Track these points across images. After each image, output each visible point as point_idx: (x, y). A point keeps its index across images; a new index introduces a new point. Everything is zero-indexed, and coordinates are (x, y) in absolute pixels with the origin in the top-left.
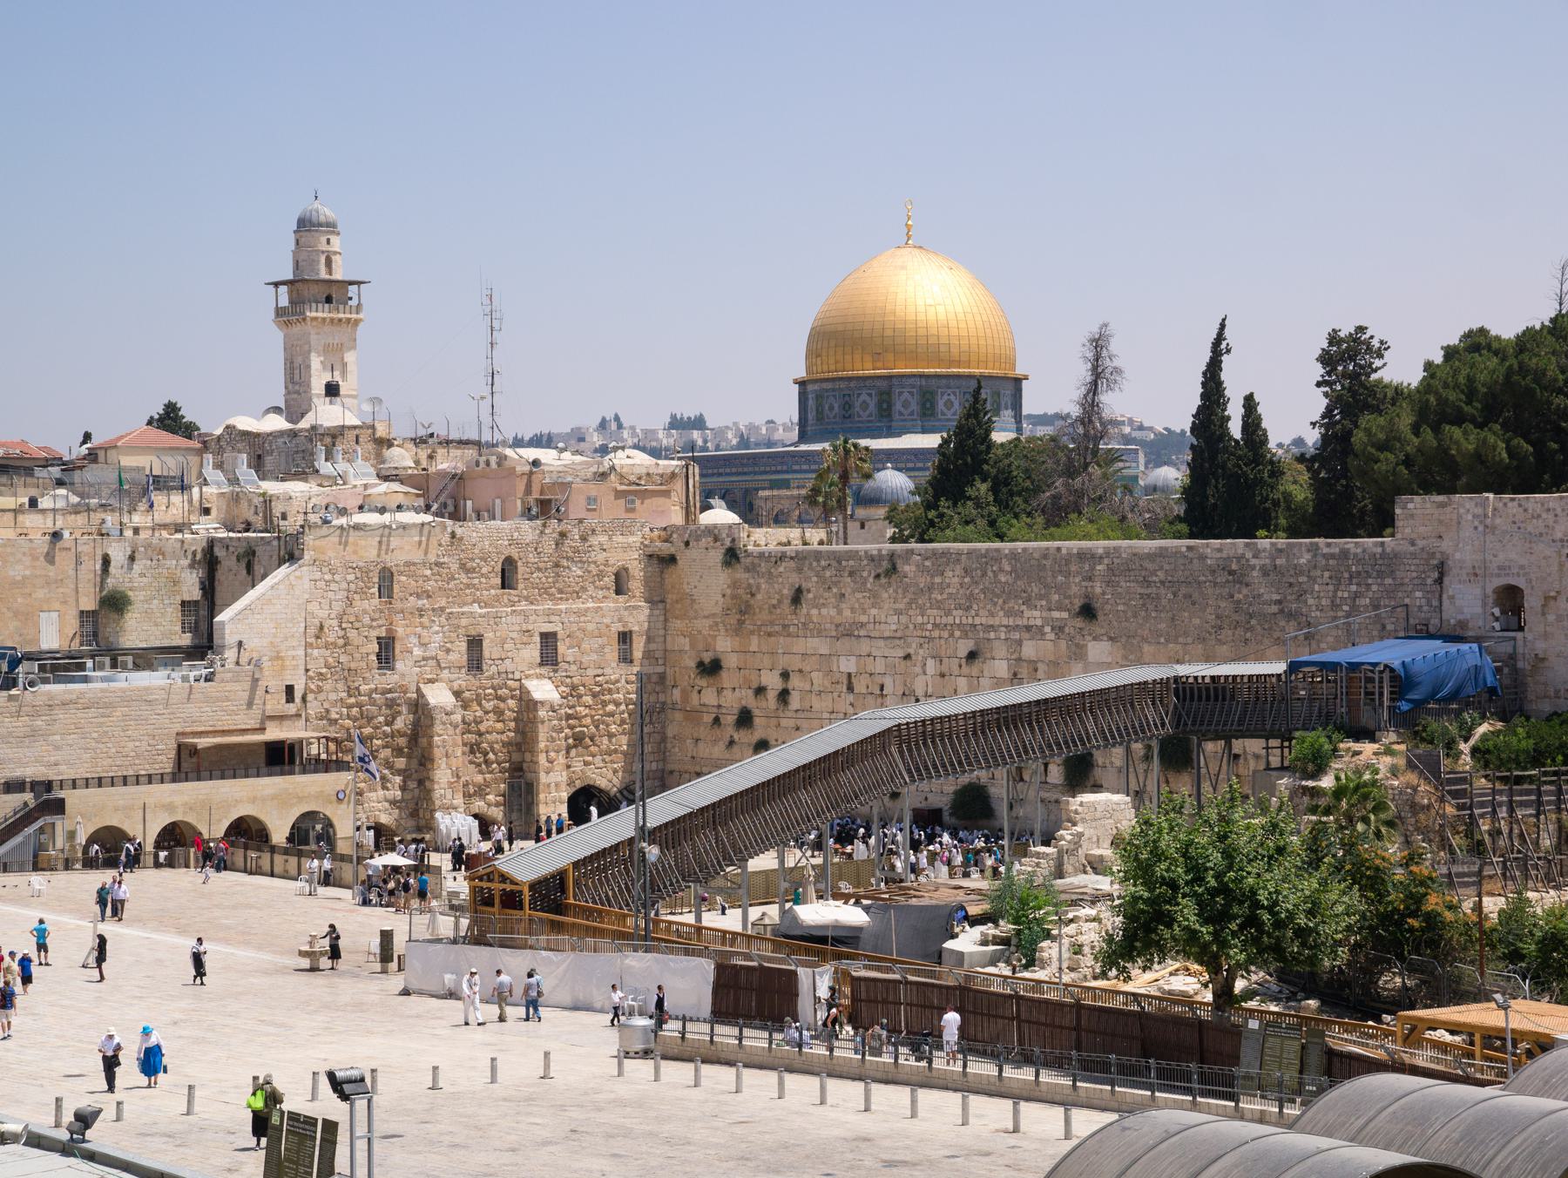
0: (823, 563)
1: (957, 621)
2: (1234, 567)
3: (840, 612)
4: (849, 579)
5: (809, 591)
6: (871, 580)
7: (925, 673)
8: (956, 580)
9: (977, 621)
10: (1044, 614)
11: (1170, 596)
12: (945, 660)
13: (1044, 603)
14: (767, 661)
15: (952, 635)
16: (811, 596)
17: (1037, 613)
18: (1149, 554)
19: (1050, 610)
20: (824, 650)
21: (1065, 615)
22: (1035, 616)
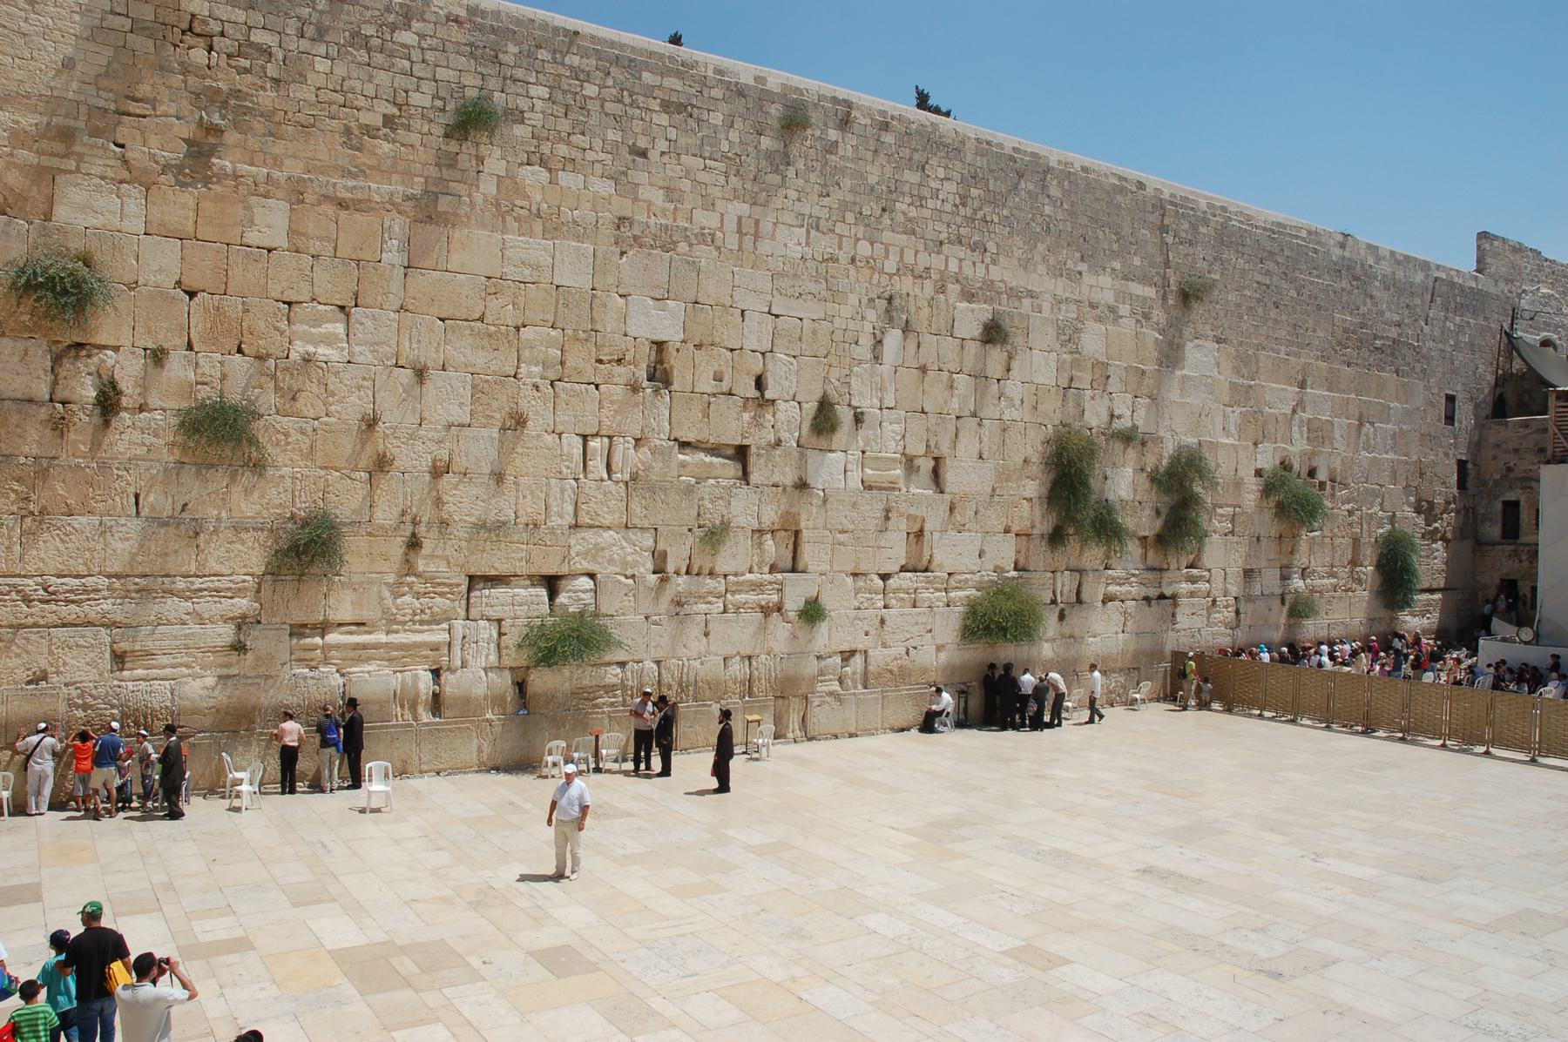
0: (575, 60)
1: (953, 266)
2: (1358, 271)
3: (632, 191)
4: (663, 119)
5: (518, 116)
6: (734, 136)
7: (877, 358)
8: (951, 187)
9: (995, 273)
10: (1119, 284)
11: (1293, 293)
12: (929, 340)
13: (1117, 265)
14: (331, 283)
15: (942, 289)
16: (520, 131)
17: (1106, 280)
18: (1265, 229)
19: (1126, 278)
20: (574, 276)
21: (1150, 292)
22: (1102, 286)
